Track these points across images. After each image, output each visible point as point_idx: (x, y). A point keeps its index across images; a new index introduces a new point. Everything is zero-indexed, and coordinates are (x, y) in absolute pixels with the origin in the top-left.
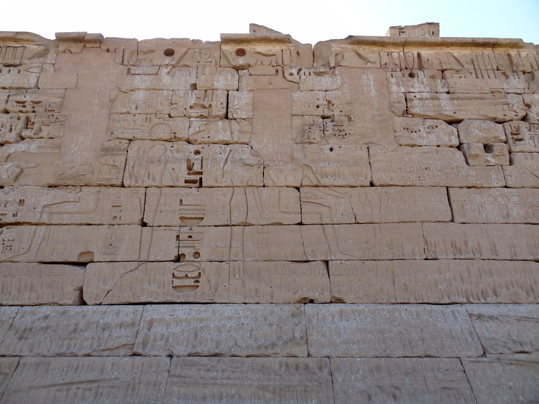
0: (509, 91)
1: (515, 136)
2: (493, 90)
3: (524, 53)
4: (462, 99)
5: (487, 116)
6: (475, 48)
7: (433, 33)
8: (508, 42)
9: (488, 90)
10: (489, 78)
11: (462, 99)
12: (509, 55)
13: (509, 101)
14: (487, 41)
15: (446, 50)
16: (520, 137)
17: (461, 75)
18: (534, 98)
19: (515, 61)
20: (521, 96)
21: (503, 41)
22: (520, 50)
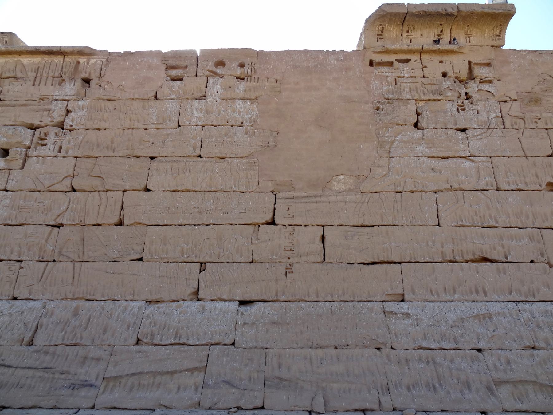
0: (57, 98)
1: (40, 142)
2: (42, 97)
3: (92, 61)
4: (7, 106)
5: (23, 122)
6: (47, 56)
7: (6, 42)
8: (71, 50)
9: (37, 97)
10: (45, 85)
11: (7, 106)
12: (78, 62)
13: (52, 107)
14: (49, 49)
15: (18, 58)
16: (44, 142)
17: (18, 83)
18: (78, 105)
19: (81, 67)
20: (66, 103)
21: (66, 50)
22: (91, 57)
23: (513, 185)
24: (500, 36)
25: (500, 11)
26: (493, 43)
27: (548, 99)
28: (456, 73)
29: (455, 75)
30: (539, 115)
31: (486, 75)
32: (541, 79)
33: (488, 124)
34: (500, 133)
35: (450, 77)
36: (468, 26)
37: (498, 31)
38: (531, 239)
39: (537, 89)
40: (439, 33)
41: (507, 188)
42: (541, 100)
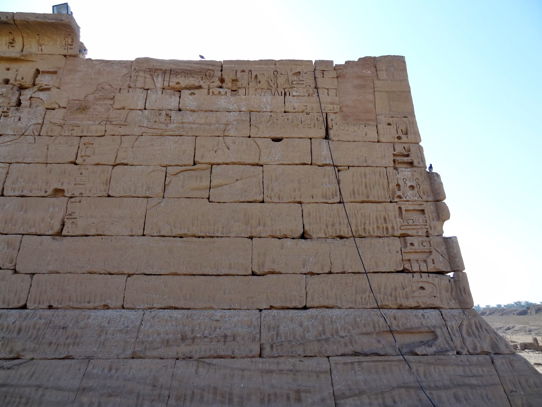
23: (19, 191)
24: (72, 45)
25: (53, 21)
26: (65, 52)
27: (97, 107)
28: (19, 81)
29: (18, 82)
30: (79, 122)
31: (46, 83)
32: (99, 87)
33: (24, 131)
34: (30, 139)
35: (11, 84)
36: (38, 35)
37: (70, 41)
38: (9, 245)
39: (91, 98)
40: (11, 41)
41: (10, 194)
42: (90, 108)
